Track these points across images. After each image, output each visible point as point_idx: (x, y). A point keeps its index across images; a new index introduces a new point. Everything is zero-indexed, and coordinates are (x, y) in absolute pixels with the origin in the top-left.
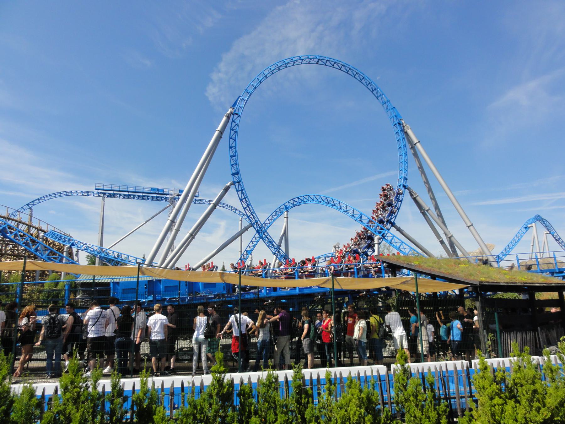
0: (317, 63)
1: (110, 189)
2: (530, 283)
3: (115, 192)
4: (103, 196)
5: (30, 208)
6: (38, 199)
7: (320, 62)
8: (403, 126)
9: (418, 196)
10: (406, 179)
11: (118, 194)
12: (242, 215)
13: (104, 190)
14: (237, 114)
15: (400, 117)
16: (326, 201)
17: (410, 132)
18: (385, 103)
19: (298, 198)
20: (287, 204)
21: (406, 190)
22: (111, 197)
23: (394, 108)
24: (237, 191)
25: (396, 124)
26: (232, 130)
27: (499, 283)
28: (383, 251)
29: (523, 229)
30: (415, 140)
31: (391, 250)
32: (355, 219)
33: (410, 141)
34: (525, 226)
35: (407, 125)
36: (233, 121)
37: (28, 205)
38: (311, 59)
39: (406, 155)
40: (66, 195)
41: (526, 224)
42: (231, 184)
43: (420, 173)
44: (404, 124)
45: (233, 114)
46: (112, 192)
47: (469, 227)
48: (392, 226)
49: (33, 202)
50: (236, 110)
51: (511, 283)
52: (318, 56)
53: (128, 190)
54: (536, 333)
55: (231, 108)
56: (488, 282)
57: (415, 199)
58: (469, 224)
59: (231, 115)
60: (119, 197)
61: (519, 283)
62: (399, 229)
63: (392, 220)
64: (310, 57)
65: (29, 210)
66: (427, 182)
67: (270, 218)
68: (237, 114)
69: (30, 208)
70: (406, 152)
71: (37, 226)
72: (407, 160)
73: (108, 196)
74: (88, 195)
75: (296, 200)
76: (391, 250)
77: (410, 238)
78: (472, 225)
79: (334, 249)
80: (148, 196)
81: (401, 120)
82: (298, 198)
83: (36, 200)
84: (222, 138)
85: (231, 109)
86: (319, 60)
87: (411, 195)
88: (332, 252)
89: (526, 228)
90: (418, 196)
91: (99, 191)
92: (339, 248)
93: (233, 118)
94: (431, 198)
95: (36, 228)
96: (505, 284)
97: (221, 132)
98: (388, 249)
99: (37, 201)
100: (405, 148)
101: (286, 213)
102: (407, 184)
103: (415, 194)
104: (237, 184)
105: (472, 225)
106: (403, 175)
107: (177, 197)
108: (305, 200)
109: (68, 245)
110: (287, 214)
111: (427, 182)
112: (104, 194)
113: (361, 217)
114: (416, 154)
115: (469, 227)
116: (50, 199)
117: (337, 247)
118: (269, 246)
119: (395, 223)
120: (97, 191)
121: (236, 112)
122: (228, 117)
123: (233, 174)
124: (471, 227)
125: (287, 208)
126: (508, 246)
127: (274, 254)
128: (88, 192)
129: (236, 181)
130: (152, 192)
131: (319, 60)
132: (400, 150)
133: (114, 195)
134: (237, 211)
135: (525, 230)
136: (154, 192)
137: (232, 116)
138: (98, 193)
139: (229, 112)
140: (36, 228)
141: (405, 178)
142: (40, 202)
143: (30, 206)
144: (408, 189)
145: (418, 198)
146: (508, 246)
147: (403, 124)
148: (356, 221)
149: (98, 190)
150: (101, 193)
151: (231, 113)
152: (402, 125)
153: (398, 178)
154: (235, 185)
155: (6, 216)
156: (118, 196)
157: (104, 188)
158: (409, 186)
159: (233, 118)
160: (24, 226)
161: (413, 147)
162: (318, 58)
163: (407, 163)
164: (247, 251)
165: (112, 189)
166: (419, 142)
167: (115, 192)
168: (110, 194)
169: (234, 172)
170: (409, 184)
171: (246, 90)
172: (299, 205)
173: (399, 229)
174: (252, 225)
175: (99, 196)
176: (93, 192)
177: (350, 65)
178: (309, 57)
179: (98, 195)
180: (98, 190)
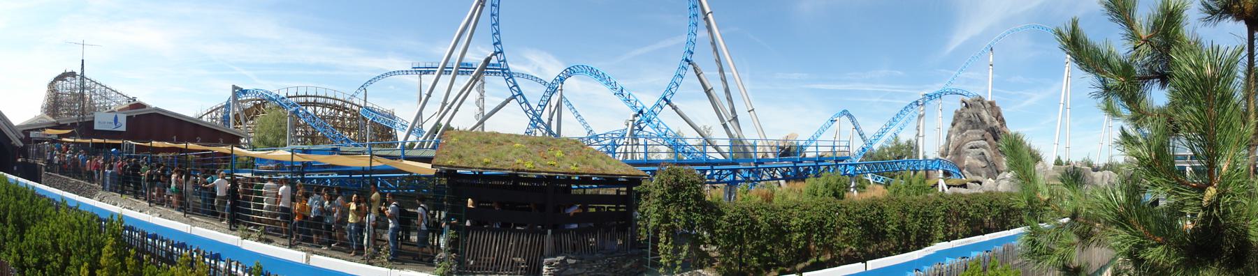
10: (692, 53)
19: (569, 68)
20: (562, 75)
21: (691, 66)
29: (829, 122)
32: (614, 92)
43: (711, 49)
47: (749, 111)
57: (698, 76)
58: (751, 109)
61: (509, 170)
62: (675, 108)
63: (668, 98)
66: (719, 61)
67: (548, 90)
75: (568, 70)
77: (687, 119)
82: (569, 68)
87: (696, 72)
94: (722, 79)
101: (560, 85)
103: (700, 70)
105: (753, 110)
108: (580, 70)
110: (562, 86)
111: (719, 61)
114: (709, 28)
115: (749, 111)
119: (670, 101)
124: (752, 112)
125: (562, 81)
144: (693, 65)
145: (701, 75)
158: (694, 61)
170: (694, 59)
173: (675, 108)
174: (514, 97)
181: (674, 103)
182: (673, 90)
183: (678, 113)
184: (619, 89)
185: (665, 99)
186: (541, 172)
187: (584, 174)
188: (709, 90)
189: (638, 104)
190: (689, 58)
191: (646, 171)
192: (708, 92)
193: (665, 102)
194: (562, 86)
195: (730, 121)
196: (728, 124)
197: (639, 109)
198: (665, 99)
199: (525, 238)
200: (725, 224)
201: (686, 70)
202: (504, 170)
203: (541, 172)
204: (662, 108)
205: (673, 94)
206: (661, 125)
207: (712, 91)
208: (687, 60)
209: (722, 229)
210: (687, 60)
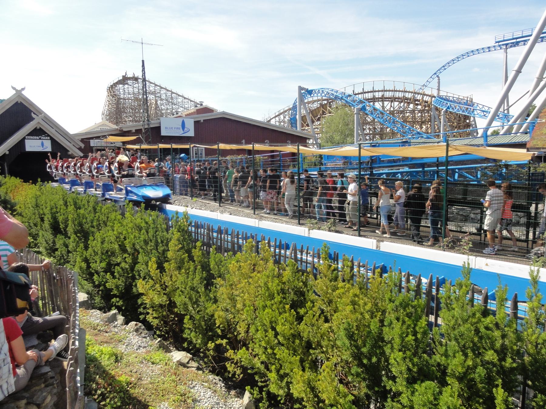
1: (511, 37)
3: (518, 40)
5: (438, 76)
6: (444, 66)
13: (504, 41)
22: (515, 46)
37: (435, 74)
40: (468, 56)
46: (515, 41)
49: (439, 70)
65: (437, 78)
69: (438, 76)
71: (430, 94)
73: (511, 47)
74: (489, 51)
83: (441, 68)
91: (500, 43)
95: (430, 96)
109: (445, 109)
112: (507, 45)
120: (497, 44)
128: (489, 48)
140: (430, 96)
150: (503, 45)
156: (523, 43)
157: (505, 39)
165: (514, 37)
167: (518, 40)
175: (501, 48)
176: (494, 46)
179: (499, 48)
180: (499, 42)
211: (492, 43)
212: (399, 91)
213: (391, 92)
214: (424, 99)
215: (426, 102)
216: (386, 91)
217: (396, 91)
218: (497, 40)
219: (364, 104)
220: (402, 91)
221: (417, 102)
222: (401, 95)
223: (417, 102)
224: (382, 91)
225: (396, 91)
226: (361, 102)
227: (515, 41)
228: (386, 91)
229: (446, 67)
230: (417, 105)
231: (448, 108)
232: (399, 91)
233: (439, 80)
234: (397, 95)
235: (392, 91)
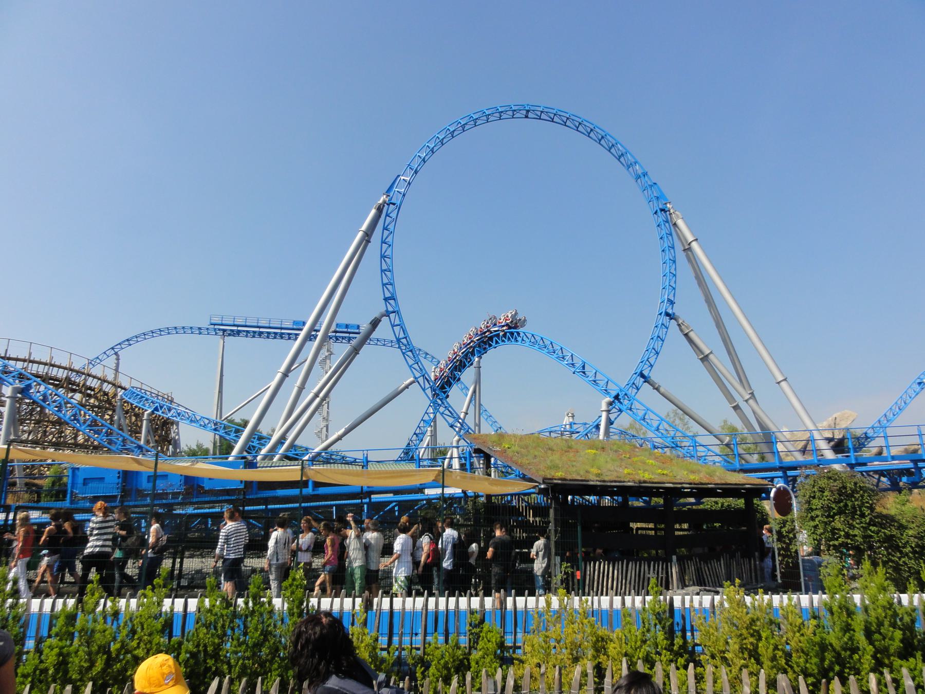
0: (527, 117)
2: (656, 483)
3: (240, 328)
4: (222, 334)
5: (116, 354)
6: (128, 340)
7: (530, 115)
8: (670, 214)
9: (692, 330)
10: (672, 302)
11: (244, 331)
12: (436, 363)
13: (222, 325)
14: (394, 204)
15: (666, 199)
16: (533, 340)
17: (680, 223)
18: (640, 177)
23: (655, 184)
24: (393, 326)
25: (657, 211)
26: (385, 228)
27: (588, 481)
28: (674, 422)
30: (690, 238)
31: (686, 421)
32: (573, 370)
33: (682, 238)
34: (919, 381)
35: (677, 212)
36: (387, 215)
37: (113, 348)
38: (502, 112)
39: (674, 262)
40: (169, 333)
41: (921, 377)
42: (383, 315)
44: (672, 211)
45: (387, 204)
46: (235, 328)
48: (645, 382)
49: (120, 344)
50: (392, 198)
51: (570, 480)
52: (528, 105)
53: (259, 325)
54: (669, 564)
55: (384, 194)
56: (564, 479)
57: (686, 335)
59: (384, 206)
60: (247, 336)
61: (629, 481)
63: (646, 373)
64: (514, 108)
65: (115, 357)
68: (394, 204)
69: (116, 354)
70: (675, 257)
72: (675, 269)
73: (230, 335)
74: (200, 333)
76: (686, 421)
78: (785, 380)
79: (566, 418)
80: (289, 334)
81: (666, 204)
83: (124, 341)
84: (370, 242)
85: (385, 196)
86: (528, 111)
88: (564, 423)
89: (919, 384)
90: (692, 330)
91: (216, 327)
92: (573, 416)
93: (388, 210)
96: (599, 483)
97: (368, 235)
98: (680, 419)
99: (127, 343)
100: (672, 251)
101: (477, 359)
102: (674, 311)
103: (687, 327)
104: (392, 316)
105: (785, 380)
106: (666, 297)
107: (334, 334)
109: (150, 411)
110: (479, 362)
112: (224, 331)
113: (584, 367)
116: (138, 341)
117: (570, 415)
118: (443, 413)
119: (650, 377)
121: (393, 201)
122: (380, 210)
123: (386, 299)
126: (885, 415)
127: (452, 426)
128: (200, 329)
129: (390, 309)
130: (295, 327)
131: (528, 111)
132: (664, 254)
133: (239, 332)
134: (428, 356)
135: (918, 388)
136: (298, 327)
137: (386, 206)
138: (215, 329)
139: (381, 201)
141: (669, 300)
142: (130, 345)
143: (116, 350)
144: (675, 319)
145: (692, 335)
146: (885, 415)
147: (669, 211)
148: (574, 373)
149: (215, 325)
150: (219, 330)
151: (384, 202)
152: (668, 213)
153: (660, 302)
154: (389, 316)
155: (68, 366)
156: (245, 333)
159: (388, 210)
160: (95, 380)
161: (688, 250)
162: (527, 108)
163: (675, 275)
164: (424, 421)
165: (236, 323)
166: (696, 240)
167: (240, 328)
168: (232, 331)
169: (388, 295)
170: (677, 310)
171: (409, 165)
172: (495, 348)
175: (216, 334)
176: (207, 329)
177: (580, 116)
178: (511, 108)
179: (214, 333)
180: (215, 325)
181: (654, 376)
182: (652, 360)
183: (663, 395)
184: (579, 364)
185: (642, 375)
186: (664, 483)
187: (709, 484)
188: (707, 356)
189: (611, 386)
190: (670, 311)
191: (765, 478)
192: (705, 359)
193: (642, 380)
194: (479, 362)
195: (746, 401)
196: (743, 405)
197: (614, 393)
198: (642, 375)
199: (646, 567)
200: (913, 542)
201: (667, 328)
202: (624, 482)
203: (664, 483)
204: (638, 389)
205: (651, 366)
206: (650, 415)
207: (711, 356)
208: (667, 314)
209: (911, 547)
210: (667, 314)
211: (205, 324)
212: (59, 367)
213: (42, 366)
214: (104, 388)
215: (106, 394)
216: (33, 362)
217: (54, 366)
218: (213, 322)
219: (28, 382)
220: (65, 368)
221: (89, 392)
222: (61, 374)
223: (89, 392)
224: (24, 361)
225: (54, 366)
226: (21, 377)
227: (235, 328)
228: (33, 362)
229: (131, 342)
230: (90, 396)
231: (156, 409)
232: (59, 367)
233: (118, 359)
234: (54, 372)
235: (46, 364)
